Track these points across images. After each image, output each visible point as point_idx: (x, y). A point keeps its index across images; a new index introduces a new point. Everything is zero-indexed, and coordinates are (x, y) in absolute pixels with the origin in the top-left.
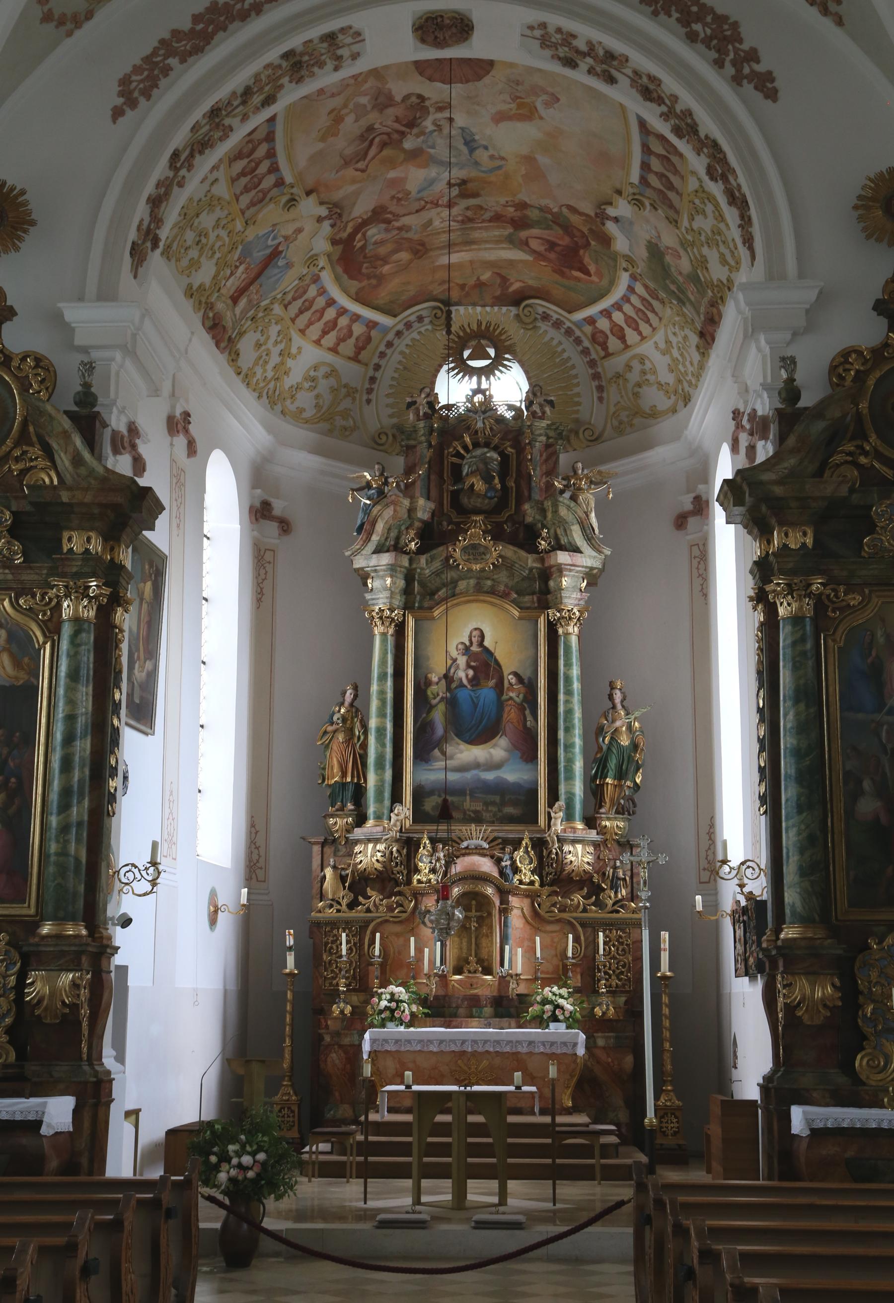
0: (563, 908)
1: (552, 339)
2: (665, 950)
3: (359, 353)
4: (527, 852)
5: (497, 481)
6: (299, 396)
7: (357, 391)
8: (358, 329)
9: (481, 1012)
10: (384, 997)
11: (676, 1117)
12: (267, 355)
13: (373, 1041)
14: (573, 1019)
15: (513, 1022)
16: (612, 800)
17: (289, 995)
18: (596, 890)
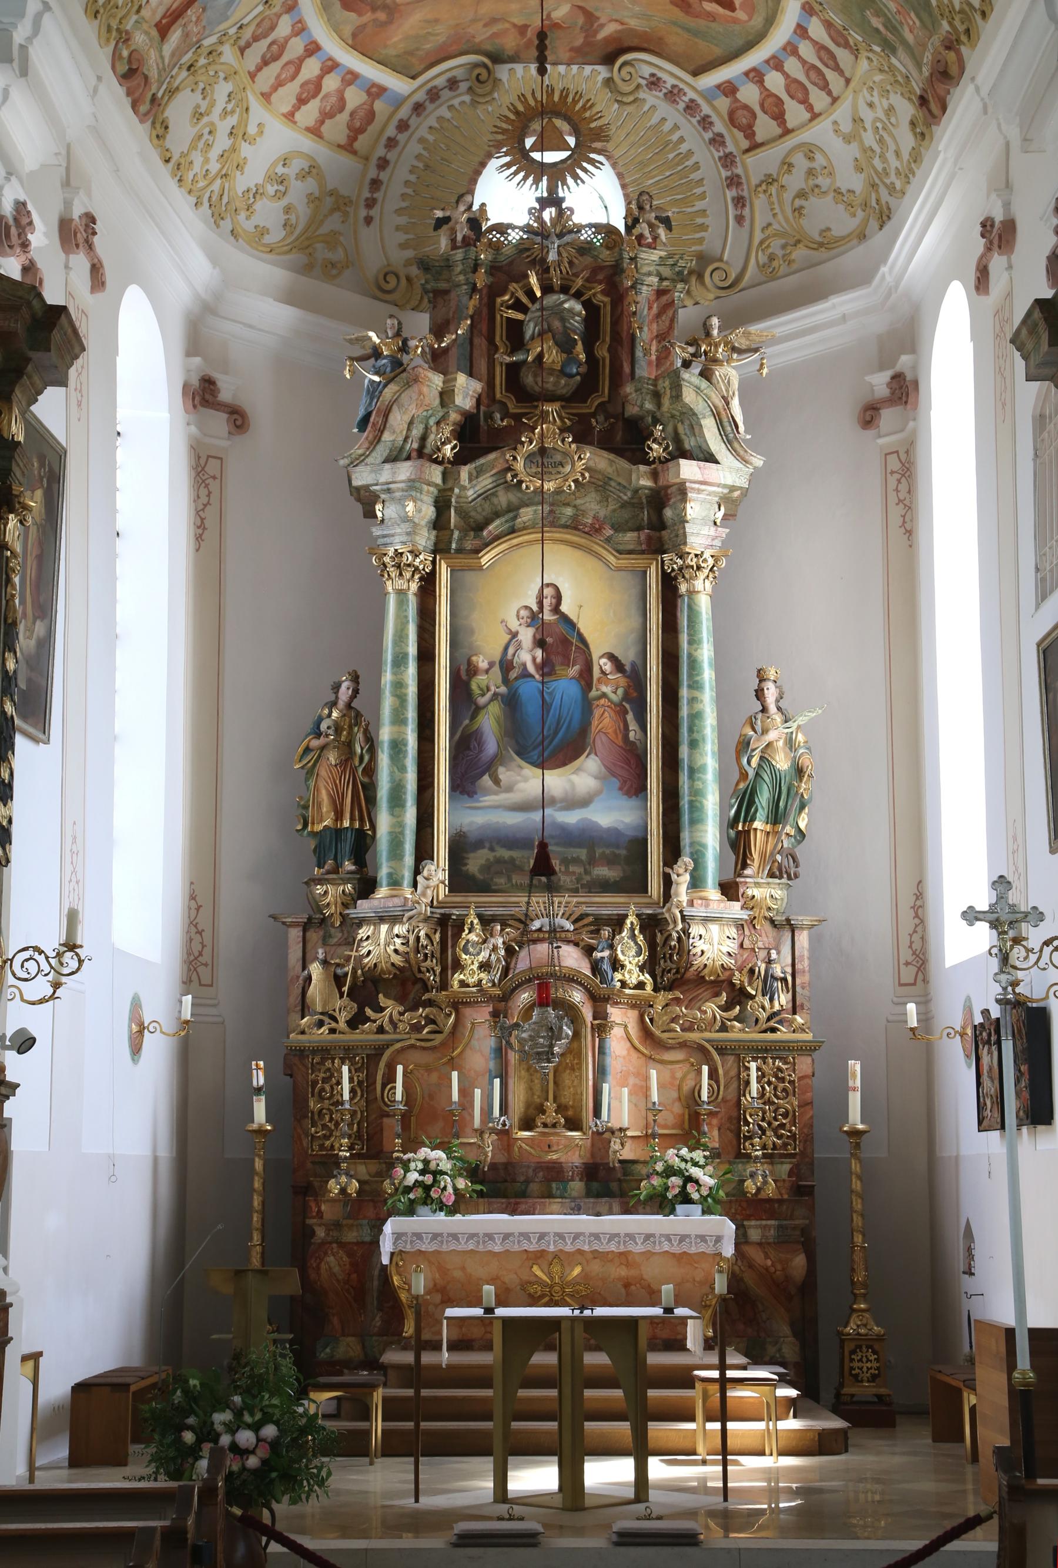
0: (687, 1025)
1: (664, 120)
2: (854, 1089)
3: (355, 139)
4: (633, 937)
5: (580, 347)
6: (258, 206)
7: (351, 202)
8: (354, 97)
9: (565, 1189)
10: (412, 1165)
11: (874, 1352)
12: (210, 132)
13: (398, 1236)
14: (714, 1199)
15: (616, 1206)
16: (763, 856)
17: (258, 1165)
18: (739, 996)
